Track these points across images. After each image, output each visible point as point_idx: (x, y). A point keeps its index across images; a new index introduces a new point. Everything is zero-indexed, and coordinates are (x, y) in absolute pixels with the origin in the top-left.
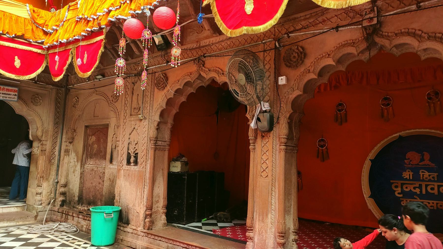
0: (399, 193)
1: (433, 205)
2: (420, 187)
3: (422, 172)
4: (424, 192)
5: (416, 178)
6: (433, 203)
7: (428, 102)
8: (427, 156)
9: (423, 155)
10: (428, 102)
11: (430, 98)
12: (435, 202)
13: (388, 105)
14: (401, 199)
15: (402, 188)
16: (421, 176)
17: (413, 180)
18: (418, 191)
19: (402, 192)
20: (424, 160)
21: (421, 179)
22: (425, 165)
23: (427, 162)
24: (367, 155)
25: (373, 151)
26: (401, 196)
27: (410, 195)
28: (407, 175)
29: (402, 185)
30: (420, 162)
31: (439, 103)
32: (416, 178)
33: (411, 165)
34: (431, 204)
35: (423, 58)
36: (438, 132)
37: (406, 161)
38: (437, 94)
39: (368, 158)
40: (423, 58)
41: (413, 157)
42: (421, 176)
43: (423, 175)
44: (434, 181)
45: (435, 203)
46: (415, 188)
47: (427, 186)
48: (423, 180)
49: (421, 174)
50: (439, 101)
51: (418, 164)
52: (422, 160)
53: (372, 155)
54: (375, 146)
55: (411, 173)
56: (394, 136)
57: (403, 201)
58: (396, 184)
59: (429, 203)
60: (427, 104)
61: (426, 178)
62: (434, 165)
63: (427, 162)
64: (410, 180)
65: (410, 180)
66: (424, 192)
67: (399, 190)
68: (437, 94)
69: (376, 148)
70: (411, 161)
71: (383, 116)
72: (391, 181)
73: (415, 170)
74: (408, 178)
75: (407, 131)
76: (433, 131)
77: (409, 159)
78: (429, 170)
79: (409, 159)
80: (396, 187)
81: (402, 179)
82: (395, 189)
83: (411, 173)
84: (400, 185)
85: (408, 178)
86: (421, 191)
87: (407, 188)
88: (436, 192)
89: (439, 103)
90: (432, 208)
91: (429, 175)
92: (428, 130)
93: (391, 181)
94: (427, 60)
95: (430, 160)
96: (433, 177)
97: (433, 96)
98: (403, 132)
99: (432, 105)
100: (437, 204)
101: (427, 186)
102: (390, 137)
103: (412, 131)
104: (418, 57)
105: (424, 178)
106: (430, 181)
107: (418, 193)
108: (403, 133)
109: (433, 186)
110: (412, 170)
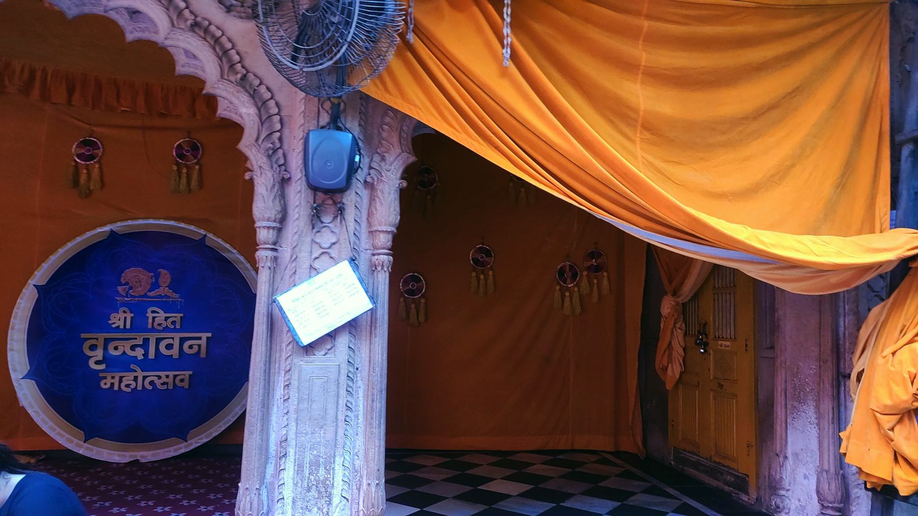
0: (97, 363)
1: (166, 380)
2: (145, 344)
3: (153, 312)
4: (152, 355)
5: (138, 325)
6: (167, 377)
7: (178, 164)
8: (165, 277)
9: (157, 276)
10: (178, 164)
11: (181, 156)
12: (171, 374)
13: (91, 157)
14: (101, 375)
15: (105, 348)
16: (150, 321)
17: (133, 329)
18: (139, 353)
19: (106, 359)
20: (159, 287)
21: (150, 326)
22: (160, 296)
23: (164, 290)
24: (30, 274)
25: (45, 265)
26: (102, 367)
27: (122, 364)
28: (120, 319)
29: (107, 341)
30: (150, 291)
31: (197, 167)
32: (138, 325)
33: (132, 296)
34: (164, 379)
35: (130, 37)
36: (192, 228)
37: (120, 288)
38: (194, 148)
39: (31, 282)
40: (130, 37)
41: (136, 278)
42: (150, 321)
43: (154, 318)
44: (175, 330)
45: (171, 377)
46: (133, 348)
47: (158, 341)
48: (153, 330)
49: (150, 315)
50: (197, 164)
51: (145, 296)
52: (155, 286)
53: (41, 275)
54: (52, 252)
55: (129, 316)
56: (99, 230)
57: (105, 378)
58: (94, 342)
59: (159, 377)
60: (175, 168)
61: (159, 325)
62: (177, 295)
63: (164, 290)
64: (125, 330)
65: (125, 330)
66: (152, 355)
67: (99, 354)
68: (194, 148)
69: (53, 258)
70: (131, 288)
71: (76, 182)
72: (83, 336)
73: (138, 309)
74: (122, 327)
75: (130, 222)
76: (183, 225)
77: (127, 284)
78: (167, 307)
79: (127, 284)
80: (93, 348)
81: (108, 328)
82: (88, 353)
83: (129, 316)
84: (101, 343)
85: (122, 327)
86: (146, 355)
87: (116, 348)
88: (175, 352)
89: (197, 167)
90: (165, 387)
91: (166, 319)
92: (172, 223)
93: (83, 336)
94: (139, 42)
95: (170, 287)
96: (173, 323)
97: (188, 151)
98: (119, 224)
99: (185, 171)
100: (175, 376)
101: (158, 341)
102: (89, 234)
103: (141, 222)
104: (121, 32)
105: (155, 324)
106: (166, 329)
107: (140, 357)
108: (117, 226)
109: (170, 341)
110: (131, 307)
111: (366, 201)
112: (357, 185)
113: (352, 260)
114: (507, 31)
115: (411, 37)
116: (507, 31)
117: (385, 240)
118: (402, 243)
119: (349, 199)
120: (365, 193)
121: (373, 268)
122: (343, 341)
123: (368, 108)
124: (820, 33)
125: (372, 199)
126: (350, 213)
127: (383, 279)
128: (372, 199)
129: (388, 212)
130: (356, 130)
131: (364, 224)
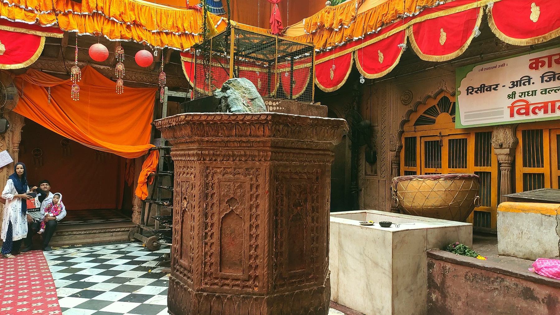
111: (11, 135)
112: (9, 131)
113: (7, 150)
114: (49, 96)
115: (23, 96)
116: (49, 96)
117: (16, 145)
118: (21, 144)
119: (6, 135)
120: (11, 134)
121: (14, 152)
122: (5, 170)
123: (11, 113)
124: (139, 95)
125: (13, 135)
126: (7, 139)
127: (16, 155)
128: (13, 135)
129: (17, 138)
130: (8, 118)
131: (11, 141)
